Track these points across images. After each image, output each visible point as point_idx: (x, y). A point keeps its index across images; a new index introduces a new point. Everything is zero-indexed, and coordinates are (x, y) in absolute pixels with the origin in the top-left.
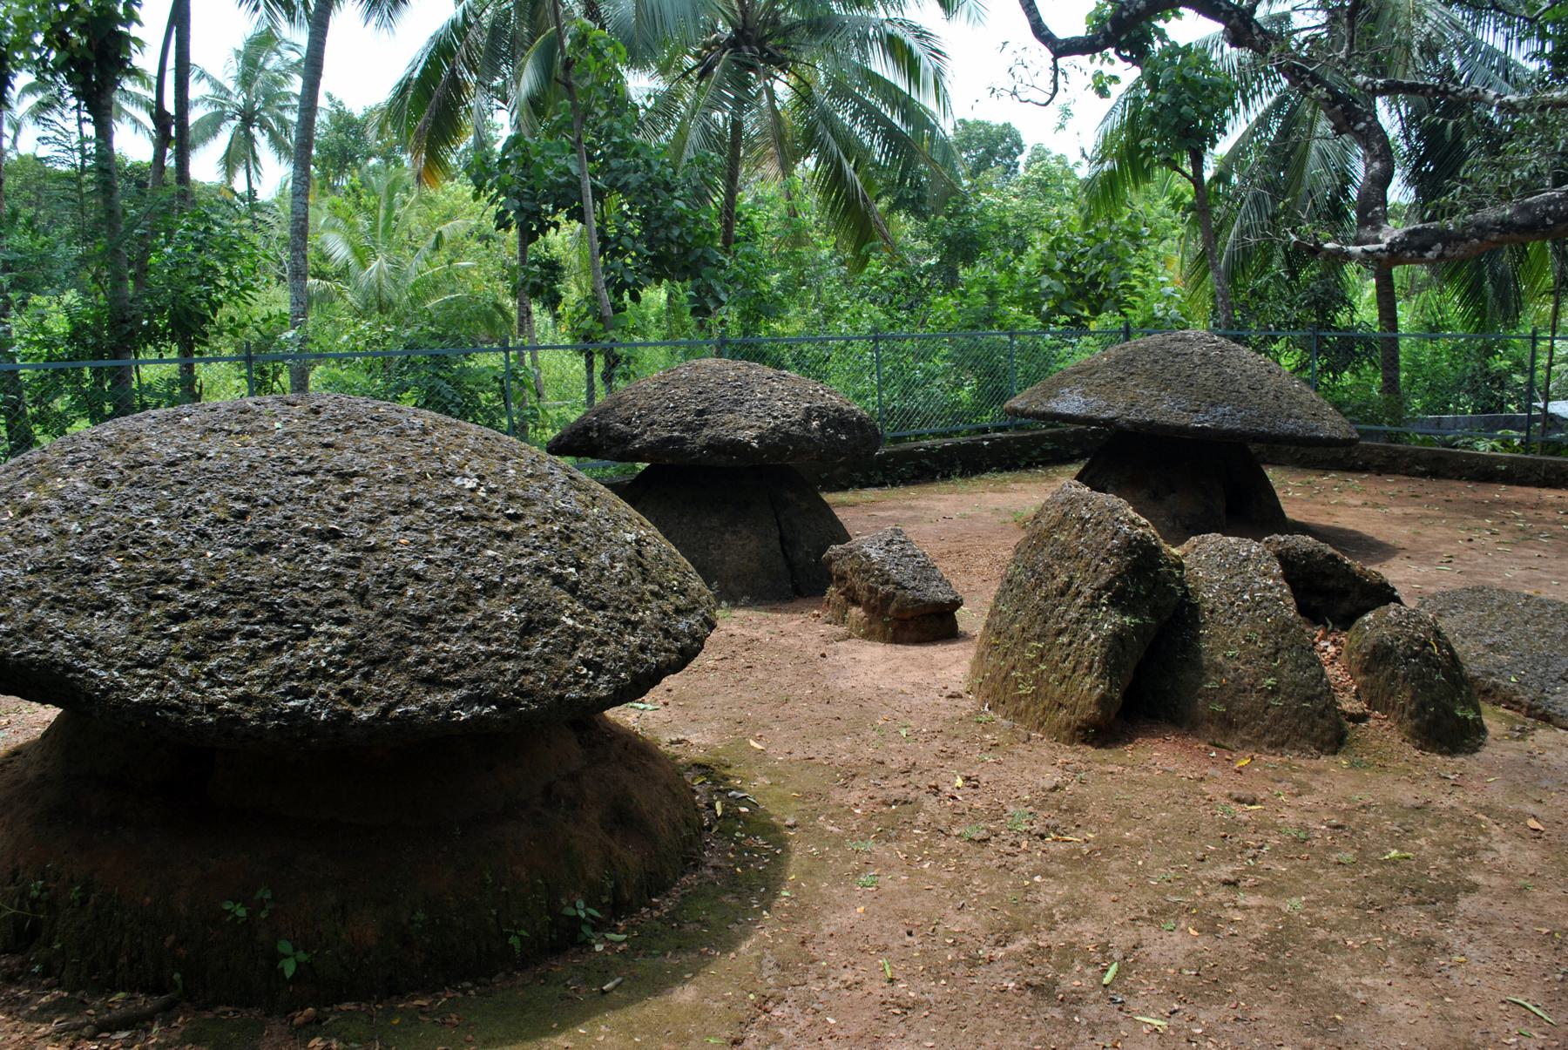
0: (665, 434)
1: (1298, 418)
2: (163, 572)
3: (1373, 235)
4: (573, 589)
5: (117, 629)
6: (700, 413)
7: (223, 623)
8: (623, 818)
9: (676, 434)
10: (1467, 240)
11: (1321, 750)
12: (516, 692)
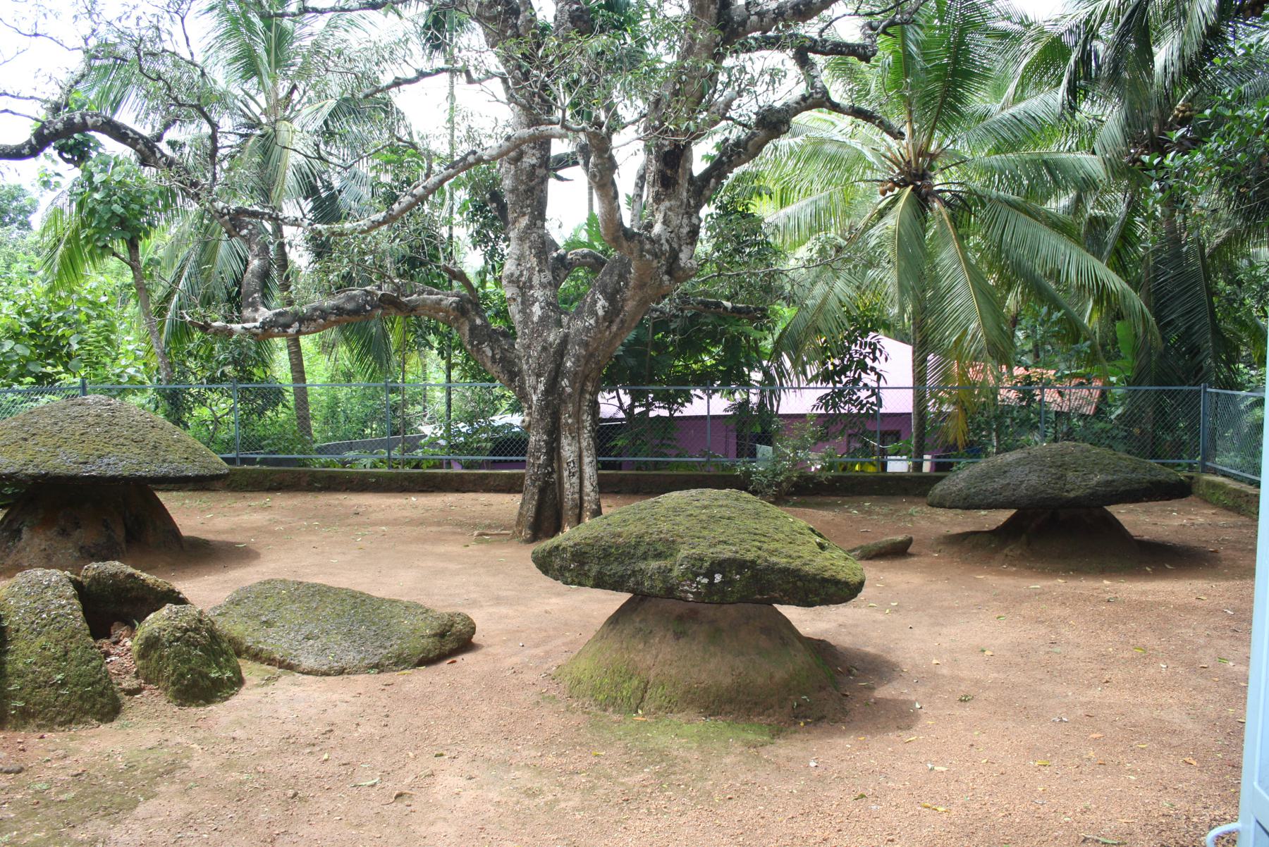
1: (171, 462)
3: (252, 315)
10: (315, 320)
11: (101, 720)
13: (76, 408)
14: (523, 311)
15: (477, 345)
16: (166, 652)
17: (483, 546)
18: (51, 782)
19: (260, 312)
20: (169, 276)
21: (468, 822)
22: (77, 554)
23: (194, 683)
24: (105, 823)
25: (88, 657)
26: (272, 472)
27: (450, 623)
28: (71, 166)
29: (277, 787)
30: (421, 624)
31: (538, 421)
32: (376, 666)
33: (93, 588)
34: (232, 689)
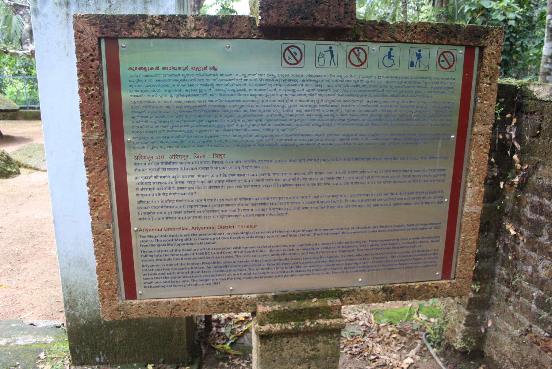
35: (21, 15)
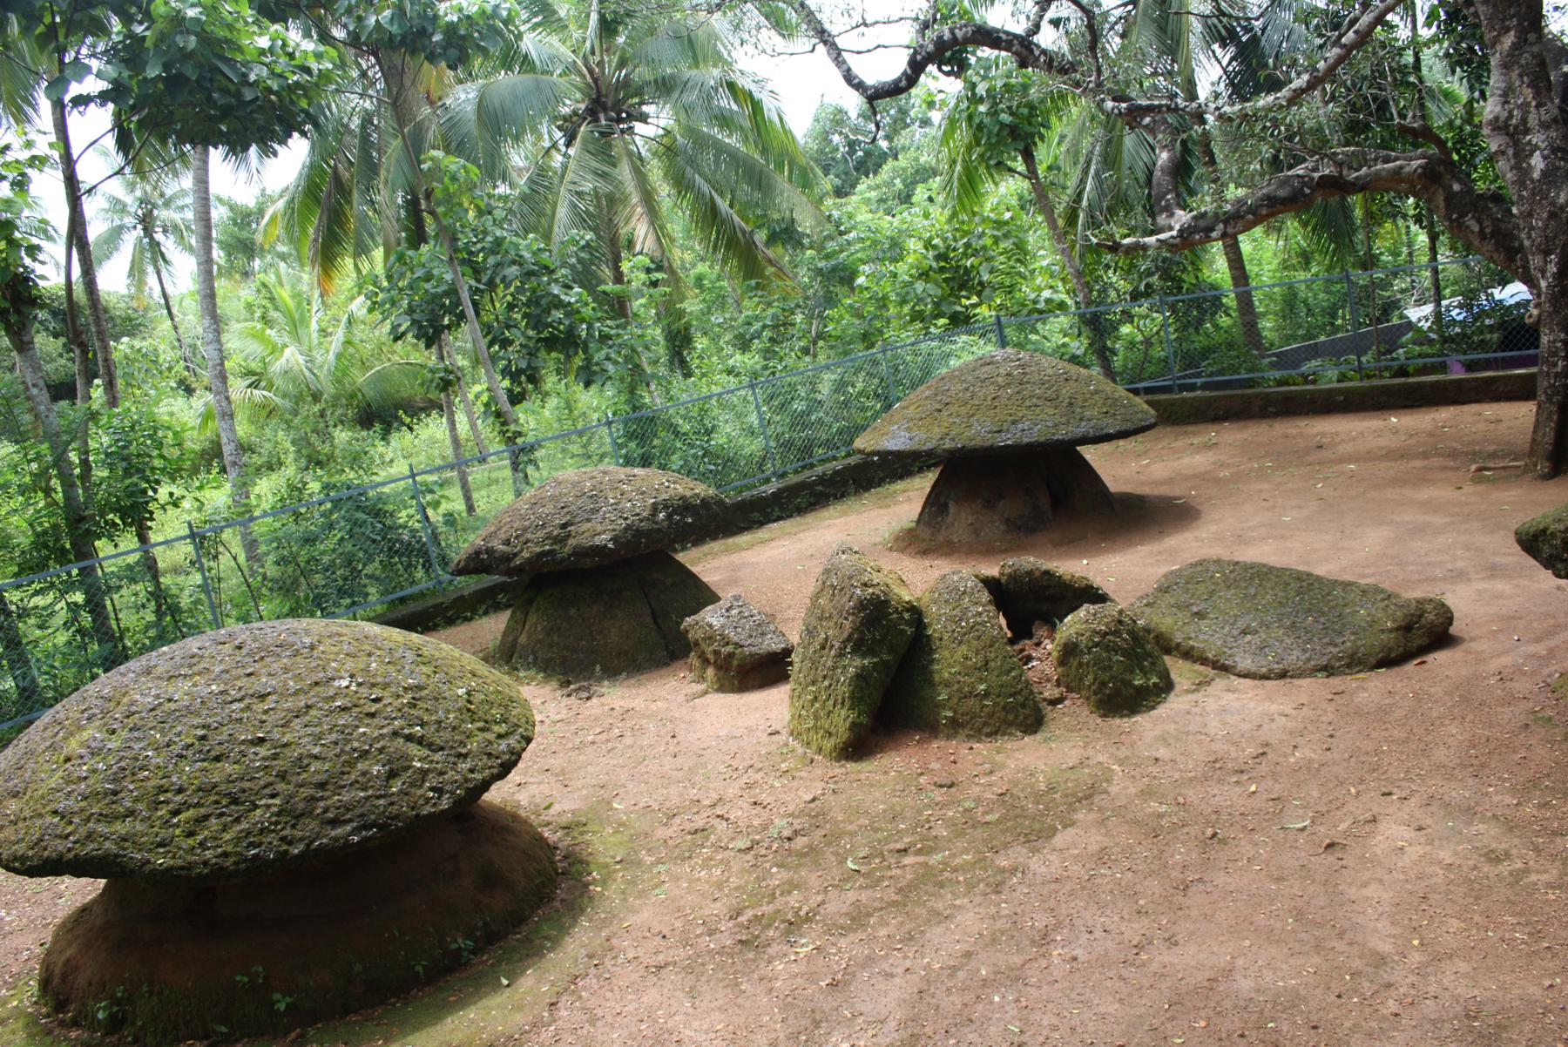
0: (538, 550)
2: (162, 786)
4: (420, 741)
5: (139, 827)
6: (564, 526)
7: (202, 811)
8: (491, 879)
9: (547, 548)
10: (1243, 217)
12: (388, 818)
13: (985, 369)
14: (1516, 167)
15: (1457, 219)
16: (1086, 658)
17: (1481, 488)
18: (978, 800)
19: (1176, 217)
20: (1072, 183)
21: (1408, 887)
22: (1003, 527)
23: (1117, 692)
24: (1025, 851)
25: (1007, 667)
26: (1216, 399)
27: (1418, 613)
28: (952, 78)
29: (1196, 823)
30: (1380, 614)
31: (1550, 315)
32: (1324, 668)
33: (1011, 586)
34: (1159, 695)
35: (1146, 127)
